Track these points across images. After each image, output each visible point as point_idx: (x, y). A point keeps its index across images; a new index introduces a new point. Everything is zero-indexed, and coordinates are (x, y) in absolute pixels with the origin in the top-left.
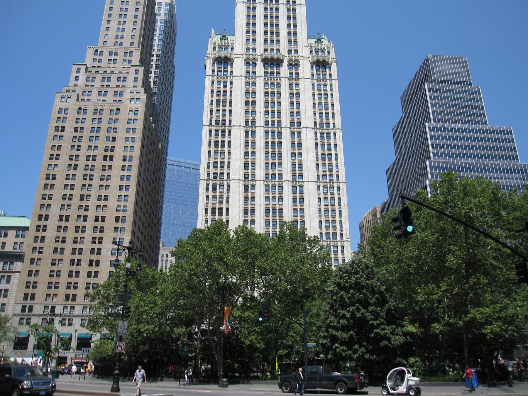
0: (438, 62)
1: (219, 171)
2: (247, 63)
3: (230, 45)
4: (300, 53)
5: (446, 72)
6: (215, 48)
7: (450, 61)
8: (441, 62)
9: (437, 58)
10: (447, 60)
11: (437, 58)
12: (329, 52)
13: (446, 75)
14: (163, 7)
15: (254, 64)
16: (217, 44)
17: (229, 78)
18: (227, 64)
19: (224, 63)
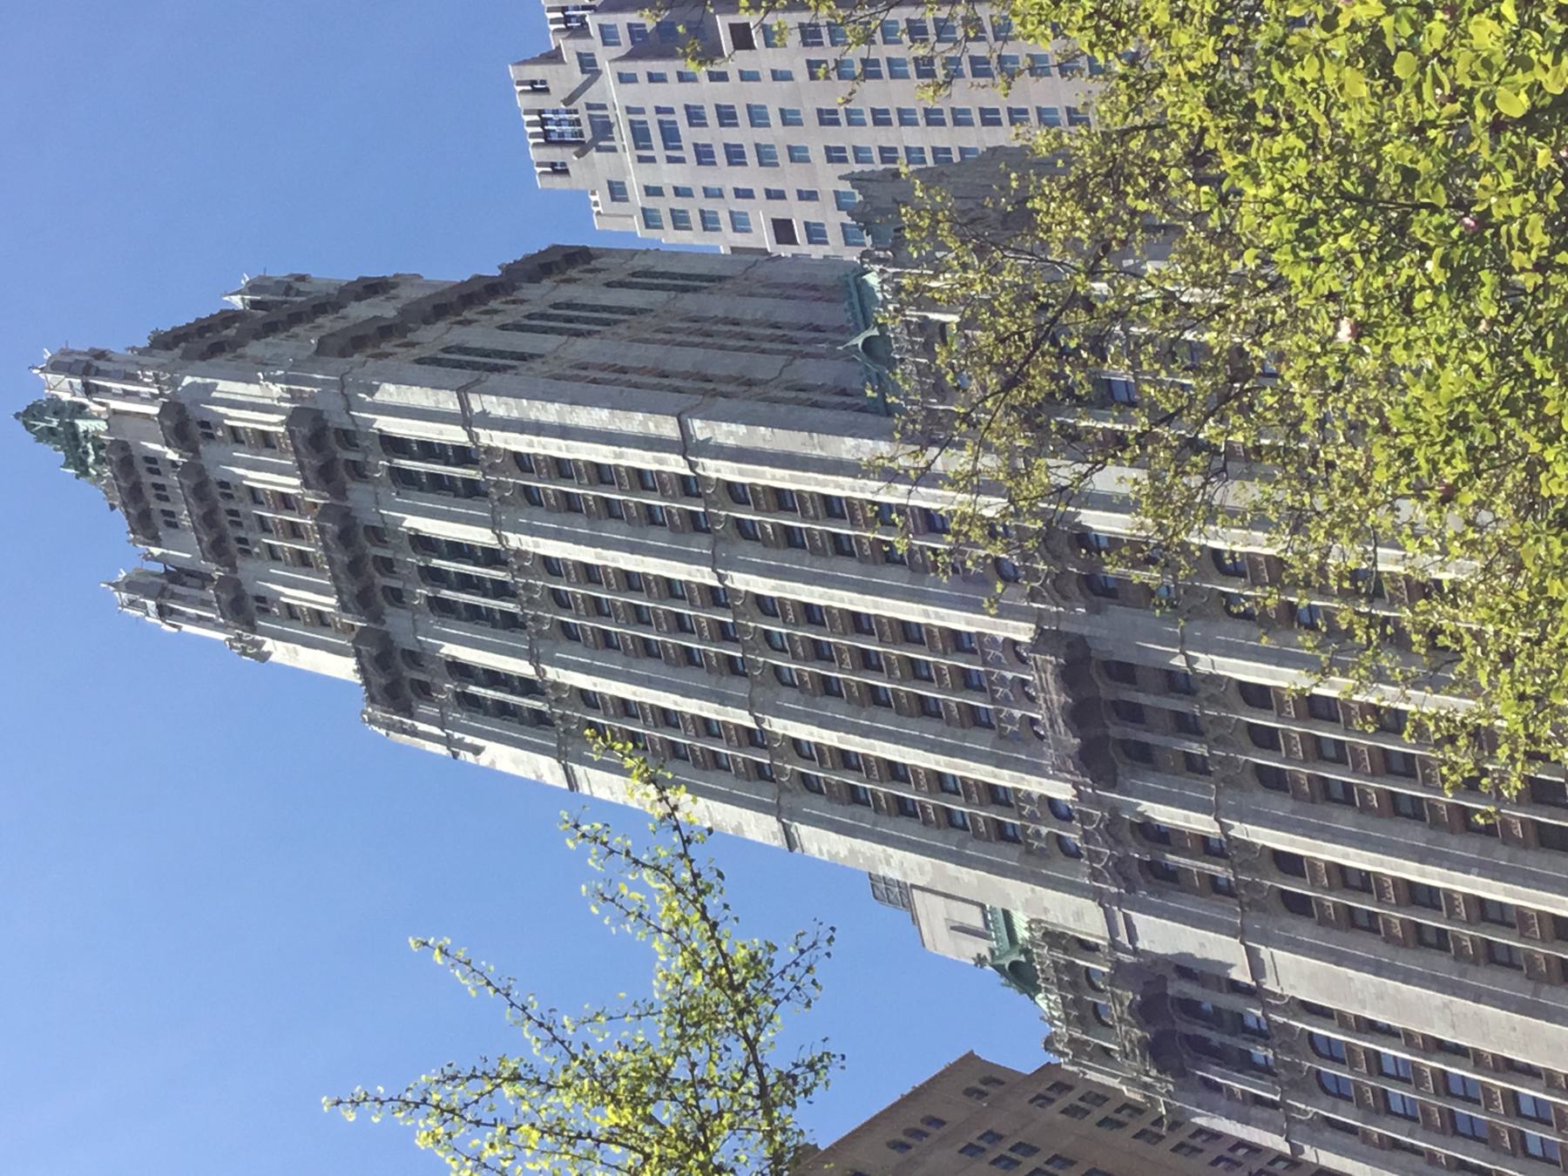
3: (1059, 955)
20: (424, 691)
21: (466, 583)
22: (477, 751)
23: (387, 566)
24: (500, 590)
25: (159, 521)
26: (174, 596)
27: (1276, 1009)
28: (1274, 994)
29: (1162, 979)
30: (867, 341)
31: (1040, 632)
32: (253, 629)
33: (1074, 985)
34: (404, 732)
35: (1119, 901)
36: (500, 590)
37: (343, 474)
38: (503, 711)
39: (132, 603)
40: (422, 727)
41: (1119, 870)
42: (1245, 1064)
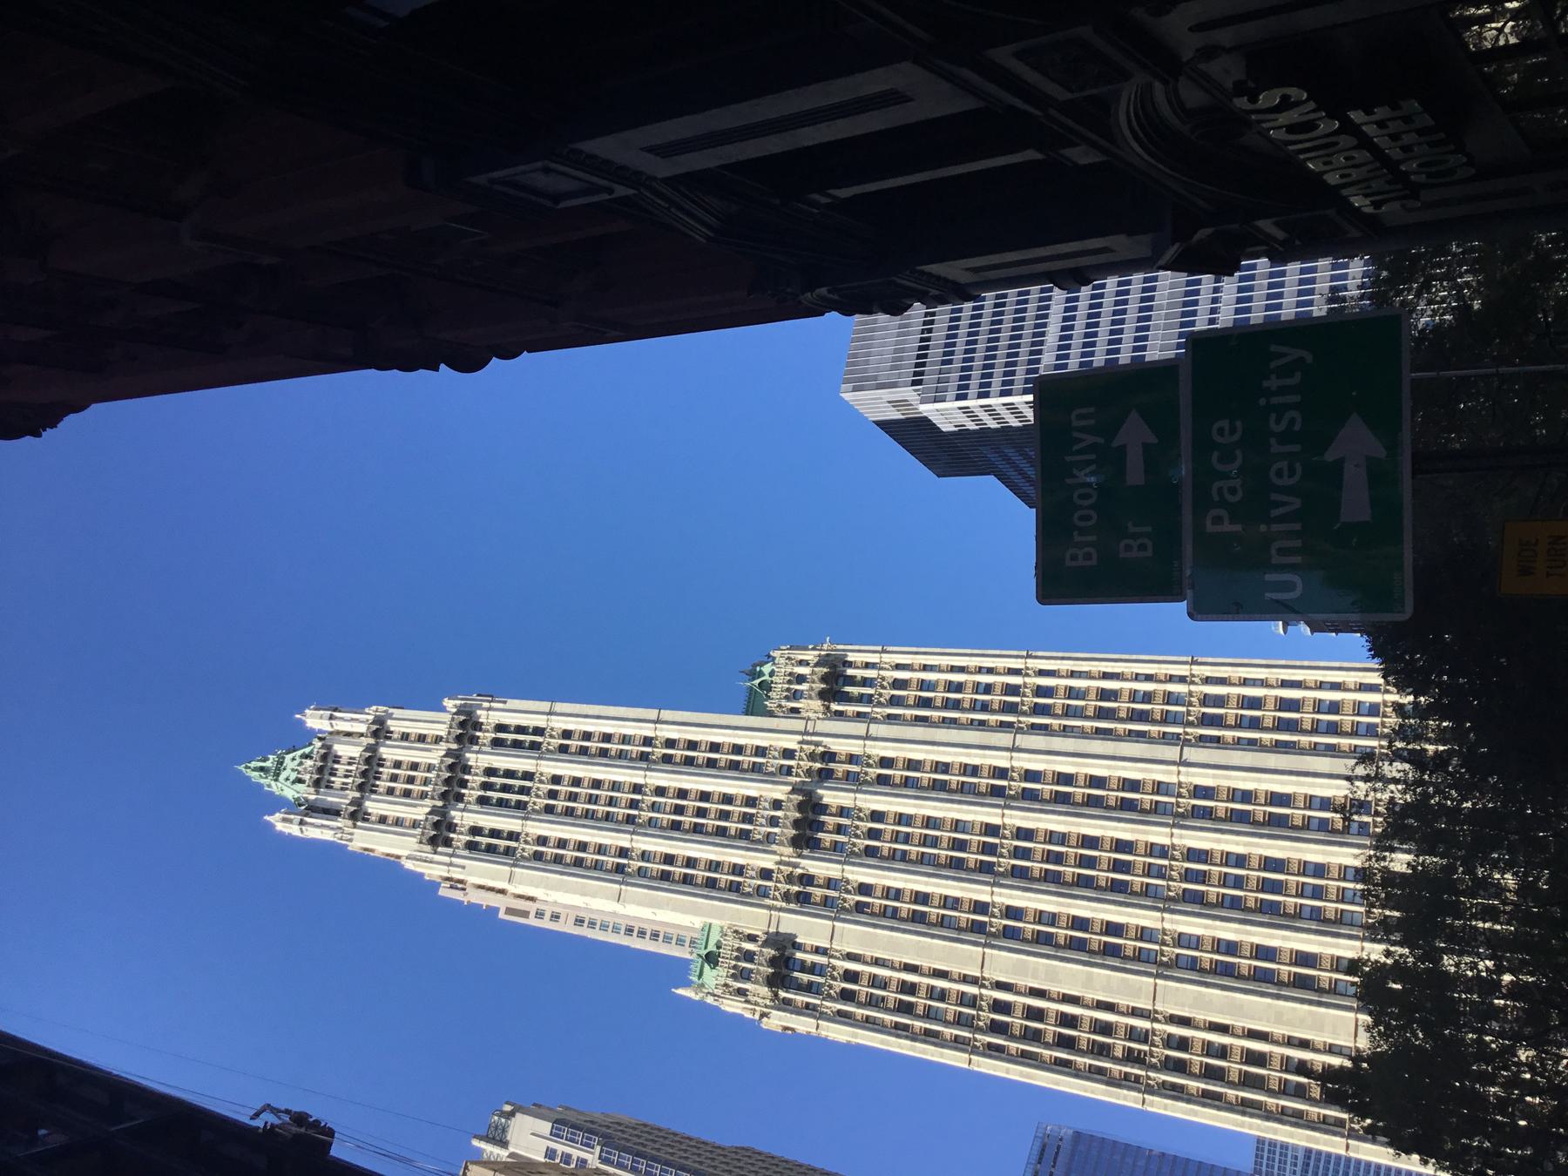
0: (865, 371)
1: (1119, 1045)
2: (803, 899)
4: (791, 743)
5: (896, 351)
6: (741, 992)
7: (864, 339)
8: (867, 362)
9: (851, 372)
10: (862, 347)
11: (851, 372)
12: (801, 663)
13: (903, 350)
14: (560, 1148)
15: (807, 879)
16: (730, 982)
17: (833, 961)
18: (792, 961)
19: (787, 967)
20: (448, 843)
21: (506, 788)
22: (463, 867)
23: (464, 784)
24: (524, 791)
25: (323, 783)
26: (311, 817)
27: (835, 957)
28: (837, 951)
29: (785, 947)
30: (760, 684)
31: (793, 789)
32: (355, 826)
33: (737, 958)
34: (426, 861)
35: (780, 909)
36: (524, 791)
37: (466, 741)
38: (491, 849)
39: (284, 820)
40: (437, 858)
41: (787, 897)
42: (809, 988)
